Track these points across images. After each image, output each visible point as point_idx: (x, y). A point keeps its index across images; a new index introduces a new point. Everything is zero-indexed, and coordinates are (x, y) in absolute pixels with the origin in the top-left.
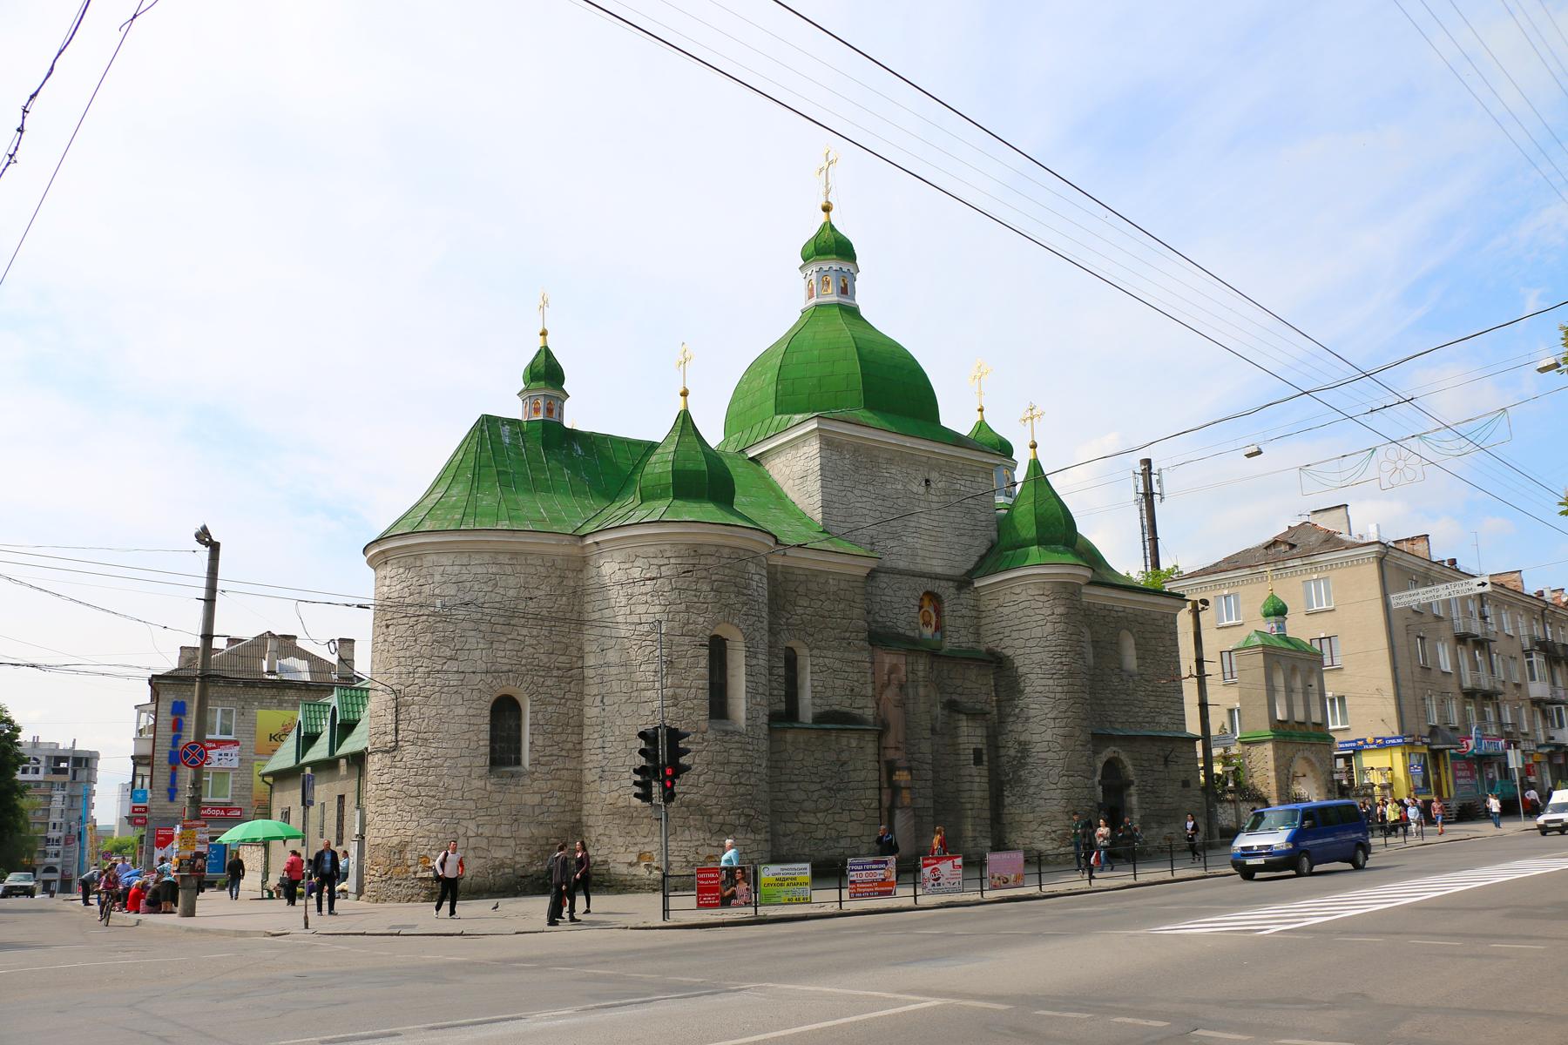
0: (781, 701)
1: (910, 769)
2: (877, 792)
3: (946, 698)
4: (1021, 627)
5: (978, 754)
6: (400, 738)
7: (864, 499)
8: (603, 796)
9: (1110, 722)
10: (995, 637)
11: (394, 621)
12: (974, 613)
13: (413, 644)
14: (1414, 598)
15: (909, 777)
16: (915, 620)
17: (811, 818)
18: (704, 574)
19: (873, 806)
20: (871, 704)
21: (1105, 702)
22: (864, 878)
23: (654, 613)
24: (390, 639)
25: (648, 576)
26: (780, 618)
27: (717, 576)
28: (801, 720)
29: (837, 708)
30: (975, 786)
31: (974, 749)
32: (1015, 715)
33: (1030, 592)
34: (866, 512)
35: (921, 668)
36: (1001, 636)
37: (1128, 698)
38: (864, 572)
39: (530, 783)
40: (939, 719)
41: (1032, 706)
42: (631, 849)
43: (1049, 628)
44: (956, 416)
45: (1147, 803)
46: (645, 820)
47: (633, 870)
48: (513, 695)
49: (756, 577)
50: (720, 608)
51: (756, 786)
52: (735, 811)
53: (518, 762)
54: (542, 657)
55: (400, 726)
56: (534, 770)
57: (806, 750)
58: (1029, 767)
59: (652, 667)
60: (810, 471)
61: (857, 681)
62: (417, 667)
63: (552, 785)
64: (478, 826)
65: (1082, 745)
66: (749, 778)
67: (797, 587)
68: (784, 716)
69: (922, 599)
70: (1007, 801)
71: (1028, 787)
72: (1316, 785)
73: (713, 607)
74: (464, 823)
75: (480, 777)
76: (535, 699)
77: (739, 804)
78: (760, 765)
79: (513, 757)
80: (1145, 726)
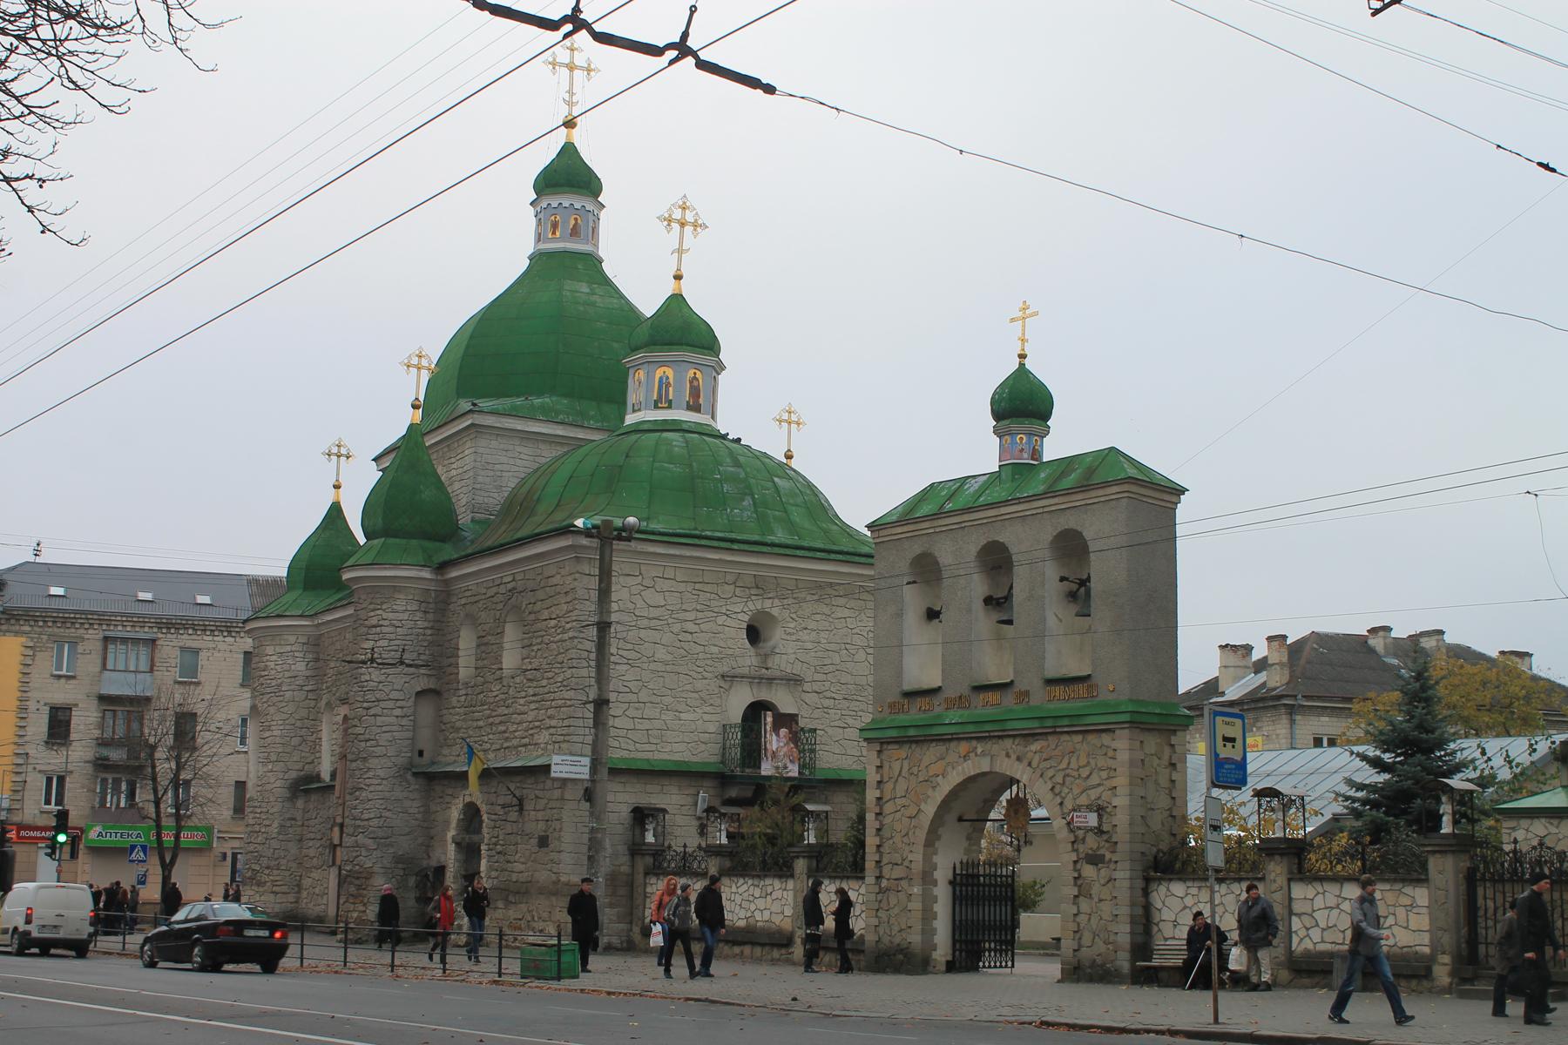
21: (481, 723)
49: (274, 658)
51: (263, 844)
66: (258, 836)
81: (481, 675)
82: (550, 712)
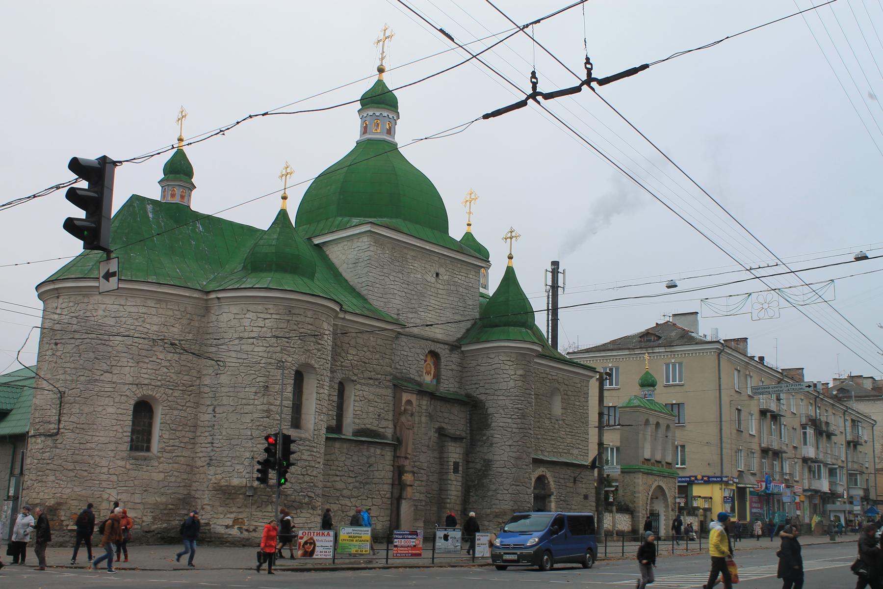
0: (334, 419)
1: (414, 473)
2: (390, 487)
3: (437, 425)
4: (492, 381)
5: (456, 465)
6: (61, 426)
7: (396, 283)
8: (210, 477)
9: (541, 451)
10: (473, 386)
11: (63, 341)
12: (460, 368)
13: (78, 359)
14: (766, 390)
15: (413, 478)
16: (422, 370)
17: (346, 502)
18: (295, 327)
19: (387, 496)
20: (391, 425)
21: (539, 437)
22: (403, 544)
23: (258, 352)
24: (59, 353)
25: (255, 325)
26: (337, 361)
27: (303, 329)
28: (344, 433)
29: (369, 426)
30: (453, 488)
31: (454, 462)
32: (483, 441)
33: (501, 358)
34: (396, 292)
35: (425, 403)
36: (477, 386)
37: (554, 435)
38: (393, 335)
39: (157, 465)
40: (432, 440)
41: (495, 436)
42: (228, 516)
43: (512, 384)
44: (456, 232)
45: (561, 508)
46: (241, 496)
47: (229, 531)
48: (148, 400)
50: (303, 352)
51: (317, 477)
52: (303, 493)
53: (148, 449)
54: (172, 375)
55: (63, 418)
56: (161, 455)
57: (347, 454)
58: (490, 478)
59: (254, 389)
60: (361, 260)
61: (383, 409)
62: (80, 376)
63: (173, 467)
64: (118, 494)
65: (526, 465)
67: (350, 340)
68: (336, 429)
69: (426, 356)
70: (472, 499)
71: (489, 490)
72: (664, 505)
73: (299, 351)
74: (108, 491)
75: (122, 459)
76: (165, 405)
77: (306, 489)
78: (319, 463)
79: (145, 445)
80: (563, 455)
81: (538, 413)
82: (578, 441)
